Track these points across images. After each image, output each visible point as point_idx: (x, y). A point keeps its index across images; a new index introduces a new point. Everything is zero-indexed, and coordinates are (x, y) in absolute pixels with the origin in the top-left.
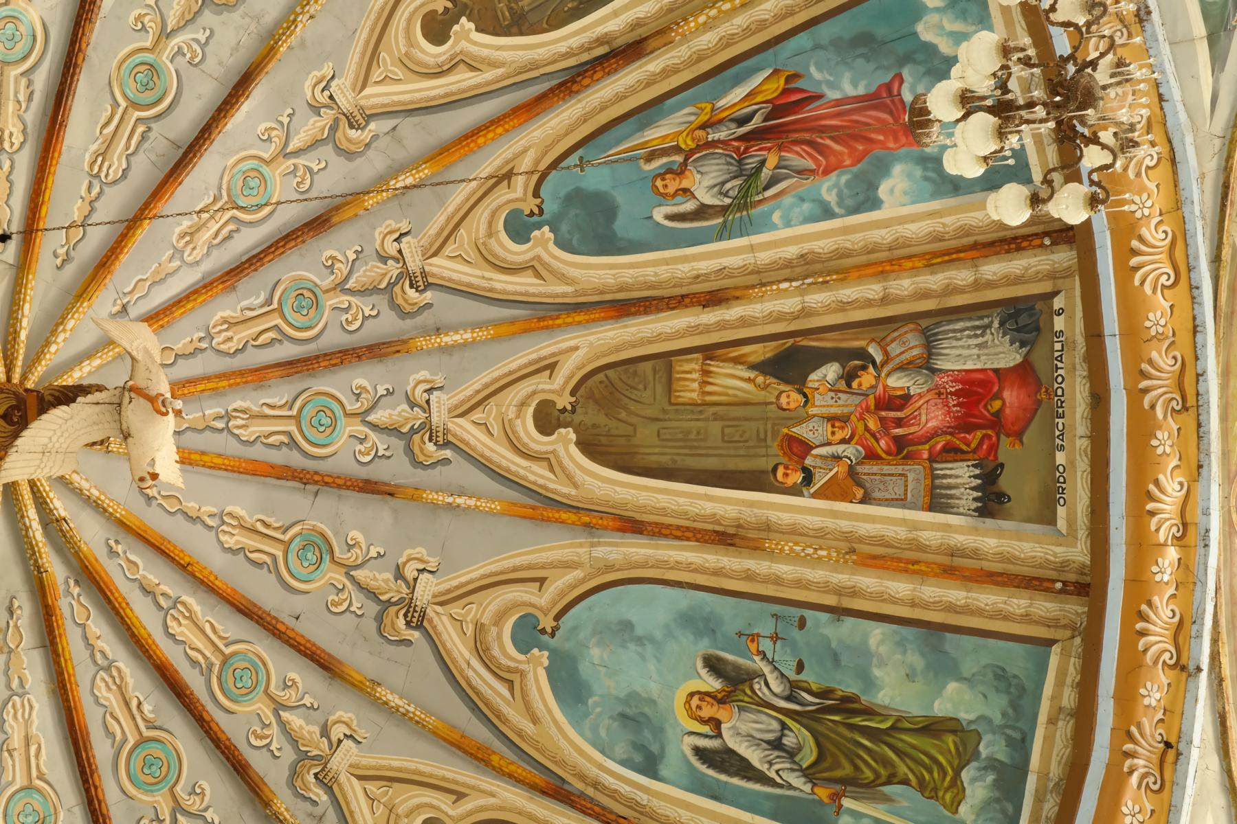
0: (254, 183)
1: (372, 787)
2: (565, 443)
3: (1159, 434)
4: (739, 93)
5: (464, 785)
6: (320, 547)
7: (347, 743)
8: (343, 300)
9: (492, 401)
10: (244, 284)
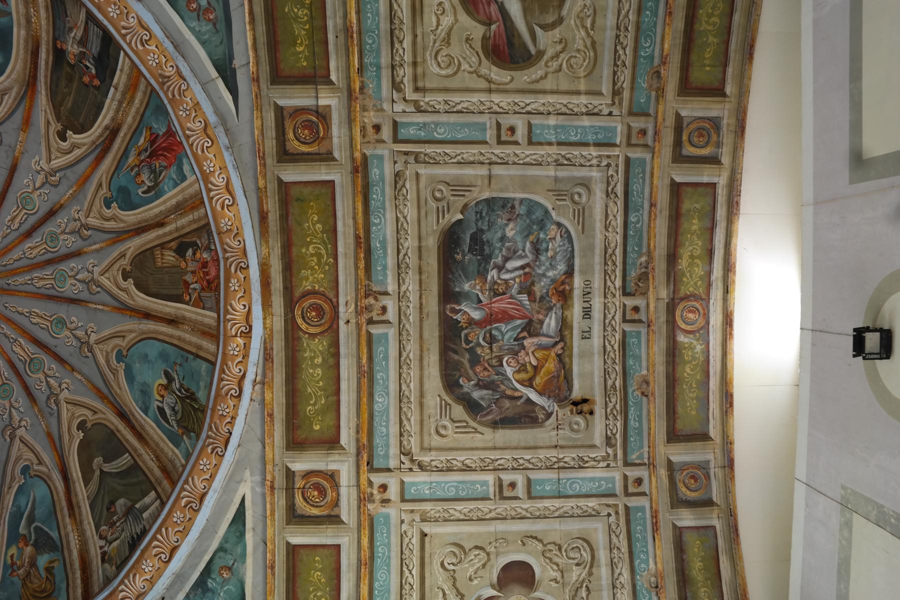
0: (29, 200)
1: (69, 406)
2: (130, 284)
3: (232, 281)
4: (142, 141)
5: (98, 409)
6: (62, 322)
7: (66, 390)
8: (66, 236)
9: (111, 269)
10: (34, 234)
